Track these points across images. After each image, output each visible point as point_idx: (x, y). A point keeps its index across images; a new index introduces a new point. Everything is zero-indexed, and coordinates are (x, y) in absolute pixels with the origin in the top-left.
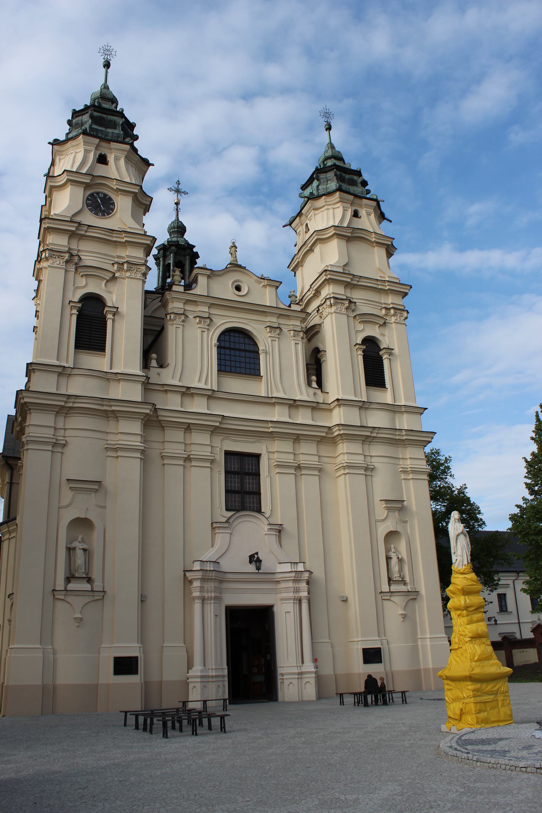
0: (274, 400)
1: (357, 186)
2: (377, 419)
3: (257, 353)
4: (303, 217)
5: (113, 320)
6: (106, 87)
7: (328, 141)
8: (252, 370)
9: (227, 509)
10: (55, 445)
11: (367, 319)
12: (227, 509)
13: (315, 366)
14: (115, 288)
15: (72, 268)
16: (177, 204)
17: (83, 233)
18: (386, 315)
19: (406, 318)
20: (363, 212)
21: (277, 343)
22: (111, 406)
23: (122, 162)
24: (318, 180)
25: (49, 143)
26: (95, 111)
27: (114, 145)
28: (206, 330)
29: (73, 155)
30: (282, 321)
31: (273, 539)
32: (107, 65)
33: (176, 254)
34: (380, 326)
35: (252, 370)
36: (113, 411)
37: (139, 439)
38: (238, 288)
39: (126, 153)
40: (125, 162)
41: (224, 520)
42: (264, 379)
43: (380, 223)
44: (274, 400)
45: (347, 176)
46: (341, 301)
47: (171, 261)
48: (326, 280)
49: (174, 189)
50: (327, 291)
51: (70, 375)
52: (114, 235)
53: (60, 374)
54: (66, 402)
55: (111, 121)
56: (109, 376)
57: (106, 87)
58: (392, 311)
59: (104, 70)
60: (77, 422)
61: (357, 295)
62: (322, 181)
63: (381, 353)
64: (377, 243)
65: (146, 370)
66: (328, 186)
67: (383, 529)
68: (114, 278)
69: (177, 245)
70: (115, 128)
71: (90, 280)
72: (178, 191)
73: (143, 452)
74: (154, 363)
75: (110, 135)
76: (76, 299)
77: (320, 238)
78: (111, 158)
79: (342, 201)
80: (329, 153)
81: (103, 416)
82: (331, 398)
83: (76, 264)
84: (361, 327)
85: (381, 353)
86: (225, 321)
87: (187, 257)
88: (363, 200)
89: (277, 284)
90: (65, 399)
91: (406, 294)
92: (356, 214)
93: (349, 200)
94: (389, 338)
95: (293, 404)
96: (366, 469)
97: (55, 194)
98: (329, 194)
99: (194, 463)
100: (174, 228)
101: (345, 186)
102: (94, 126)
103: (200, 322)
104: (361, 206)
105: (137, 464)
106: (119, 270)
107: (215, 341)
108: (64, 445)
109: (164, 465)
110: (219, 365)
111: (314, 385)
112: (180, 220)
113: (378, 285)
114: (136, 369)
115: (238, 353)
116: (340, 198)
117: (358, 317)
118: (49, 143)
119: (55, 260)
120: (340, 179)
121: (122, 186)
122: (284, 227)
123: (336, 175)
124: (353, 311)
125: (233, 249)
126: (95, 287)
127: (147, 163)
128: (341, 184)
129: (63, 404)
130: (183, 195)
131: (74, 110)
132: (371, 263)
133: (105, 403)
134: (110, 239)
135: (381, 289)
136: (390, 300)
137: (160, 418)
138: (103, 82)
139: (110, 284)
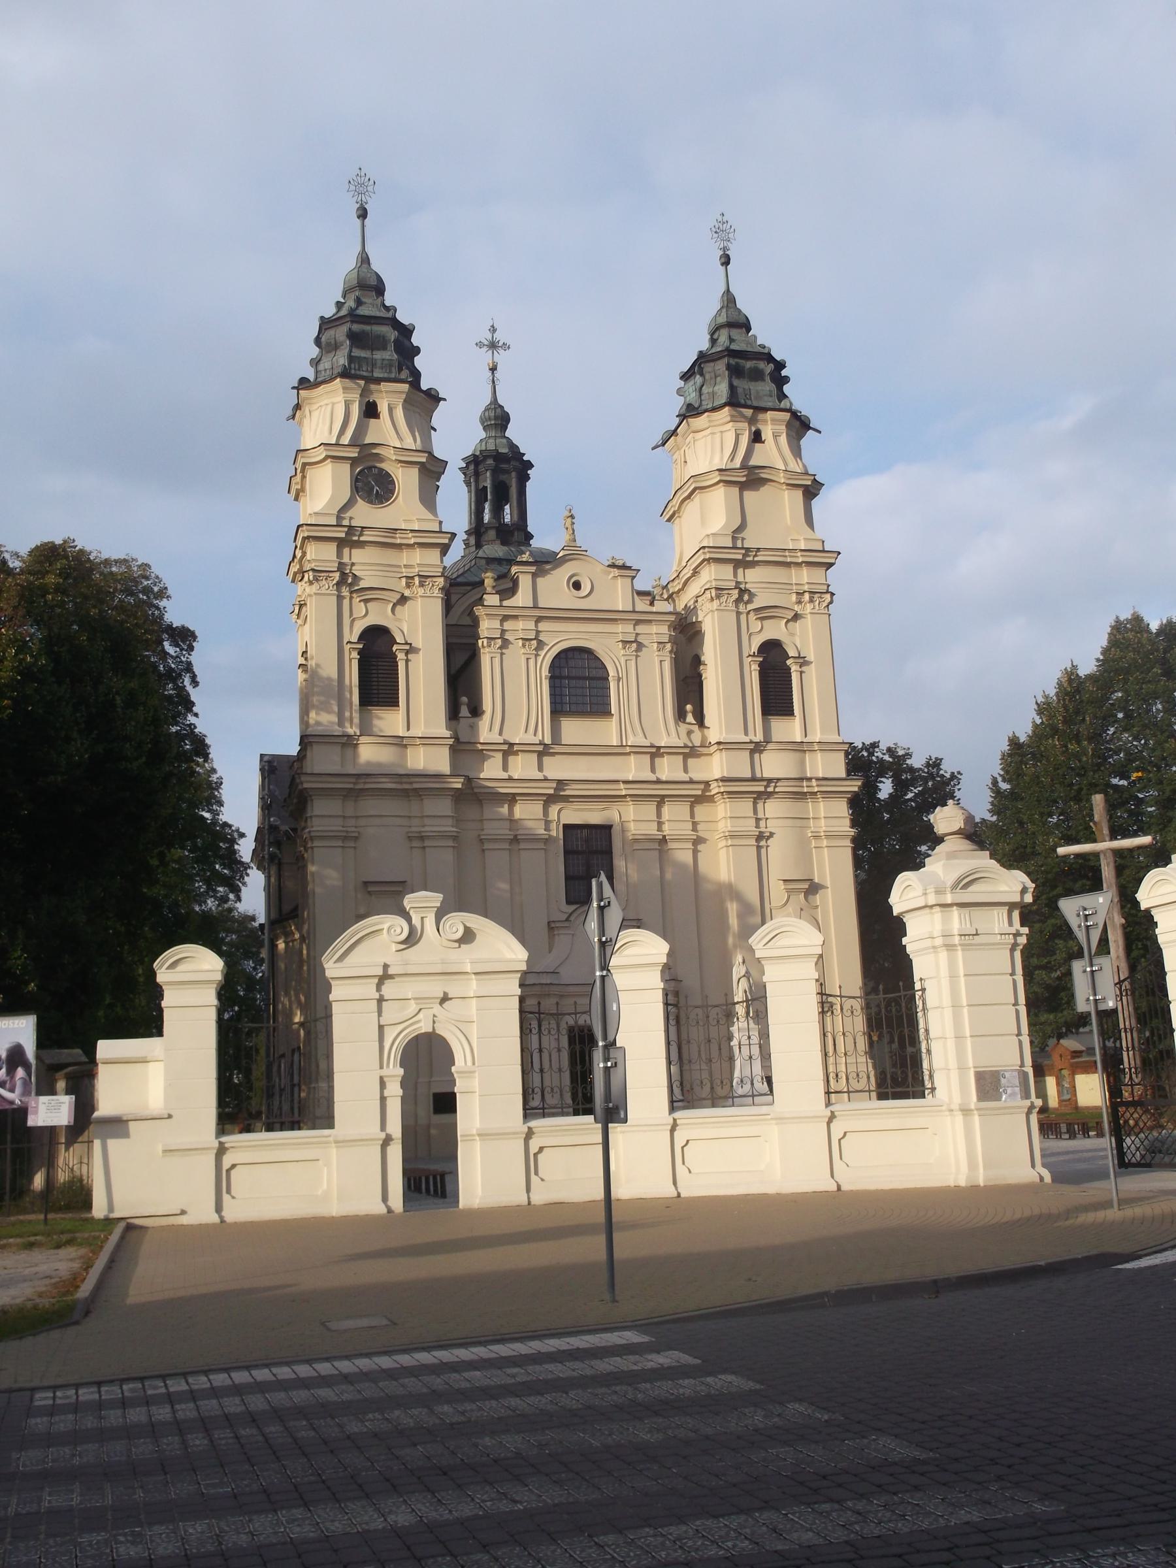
0: (628, 750)
1: (763, 380)
2: (773, 765)
3: (605, 678)
4: (679, 438)
5: (407, 661)
7: (723, 289)
8: (598, 707)
9: (569, 902)
11: (766, 613)
12: (569, 902)
13: (689, 689)
14: (404, 611)
15: (345, 592)
16: (493, 369)
19: (831, 602)
20: (767, 433)
21: (633, 662)
23: (399, 413)
24: (702, 374)
25: (293, 388)
26: (352, 322)
27: (384, 386)
29: (329, 407)
30: (641, 629)
33: (496, 472)
35: (598, 707)
36: (415, 790)
37: (450, 822)
38: (577, 586)
39: (404, 396)
40: (404, 408)
41: (564, 917)
43: (800, 436)
45: (749, 364)
47: (488, 484)
48: (704, 560)
49: (486, 343)
50: (709, 575)
53: (344, 745)
54: (355, 784)
58: (807, 597)
59: (358, 222)
60: (370, 806)
61: (752, 577)
62: (707, 376)
63: (789, 662)
64: (788, 485)
65: (454, 722)
66: (716, 388)
68: (403, 600)
69: (498, 457)
70: (384, 348)
72: (493, 346)
73: (455, 838)
74: (464, 711)
75: (379, 363)
76: (355, 639)
77: (697, 488)
78: (383, 408)
79: (733, 420)
80: (722, 319)
82: (714, 735)
83: (351, 585)
85: (789, 662)
86: (559, 637)
87: (514, 474)
89: (633, 573)
91: (831, 565)
92: (757, 437)
94: (800, 639)
95: (656, 753)
97: (310, 472)
98: (714, 409)
99: (522, 846)
100: (490, 419)
101: (741, 384)
102: (357, 353)
103: (524, 646)
105: (449, 856)
106: (408, 586)
107: (545, 672)
108: (356, 838)
109: (483, 850)
110: (553, 703)
111: (690, 718)
112: (500, 402)
114: (441, 729)
115: (578, 684)
116: (732, 416)
117: (752, 613)
118: (293, 388)
120: (735, 372)
122: (653, 449)
123: (729, 367)
124: (750, 601)
125: (569, 520)
126: (378, 616)
127: (434, 398)
128: (736, 382)
129: (351, 786)
130: (501, 351)
131: (322, 317)
132: (776, 518)
133: (404, 780)
134: (390, 541)
135: (791, 563)
136: (804, 577)
137: (476, 790)
138: (359, 248)
139: (398, 608)
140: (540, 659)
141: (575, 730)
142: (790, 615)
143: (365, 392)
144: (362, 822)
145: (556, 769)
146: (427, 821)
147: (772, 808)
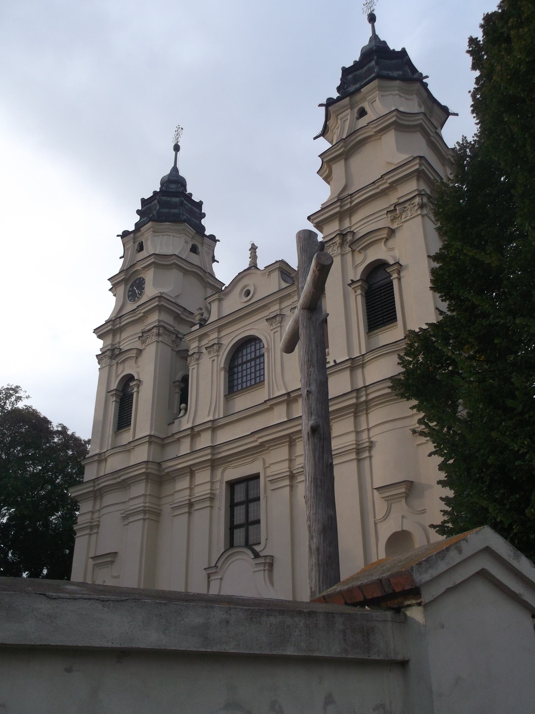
6: (175, 170)
10: (91, 528)
17: (118, 326)
18: (393, 221)
21: (279, 332)
22: (119, 477)
28: (216, 358)
31: (261, 576)
32: (177, 148)
34: (387, 239)
36: (123, 480)
38: (248, 293)
42: (266, 382)
44: (269, 403)
46: (331, 243)
51: (106, 460)
52: (137, 313)
55: (153, 205)
56: (128, 447)
57: (175, 170)
67: (386, 530)
71: (127, 364)
81: (120, 488)
84: (359, 258)
86: (230, 338)
88: (362, 90)
90: (92, 484)
93: (345, 106)
96: (358, 451)
104: (364, 99)
108: (98, 526)
113: (378, 187)
119: (103, 361)
121: (143, 264)
129: (92, 489)
137: (167, 471)
139: (140, 359)
140: (220, 358)
141: (243, 402)
142: (384, 234)
143: (134, 239)
144: (102, 512)
145: (223, 436)
146: (132, 503)
147: (376, 416)
